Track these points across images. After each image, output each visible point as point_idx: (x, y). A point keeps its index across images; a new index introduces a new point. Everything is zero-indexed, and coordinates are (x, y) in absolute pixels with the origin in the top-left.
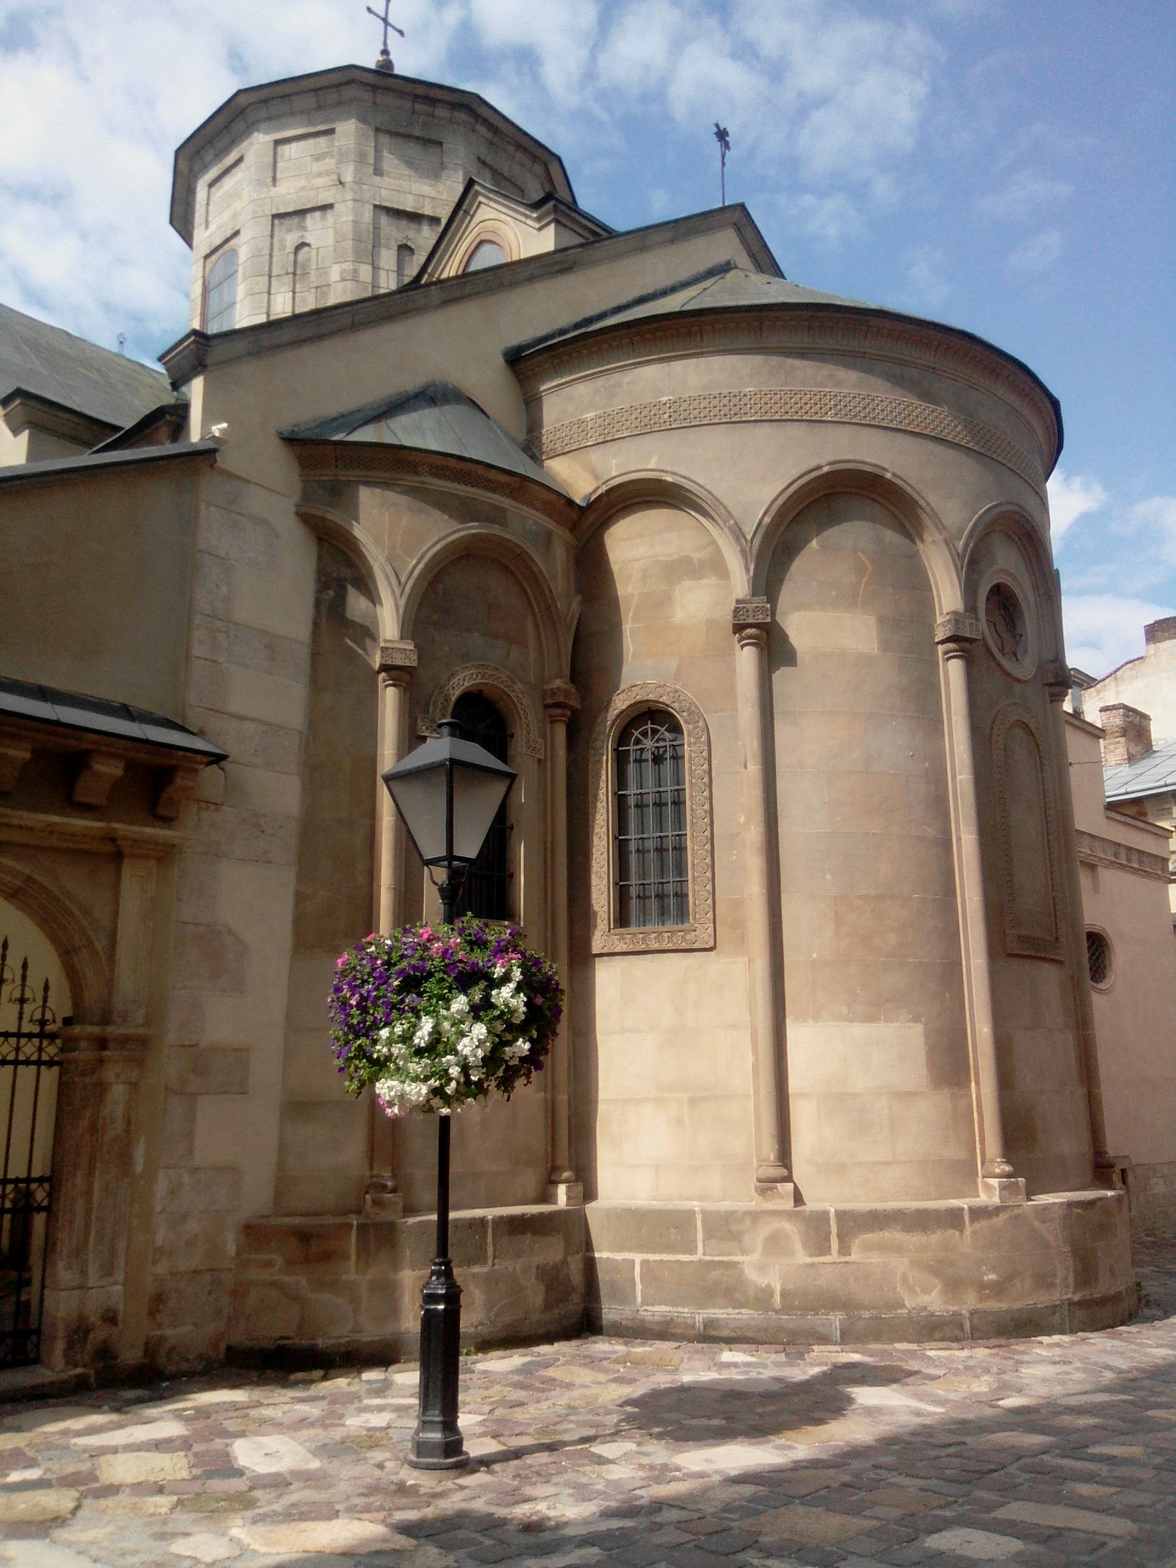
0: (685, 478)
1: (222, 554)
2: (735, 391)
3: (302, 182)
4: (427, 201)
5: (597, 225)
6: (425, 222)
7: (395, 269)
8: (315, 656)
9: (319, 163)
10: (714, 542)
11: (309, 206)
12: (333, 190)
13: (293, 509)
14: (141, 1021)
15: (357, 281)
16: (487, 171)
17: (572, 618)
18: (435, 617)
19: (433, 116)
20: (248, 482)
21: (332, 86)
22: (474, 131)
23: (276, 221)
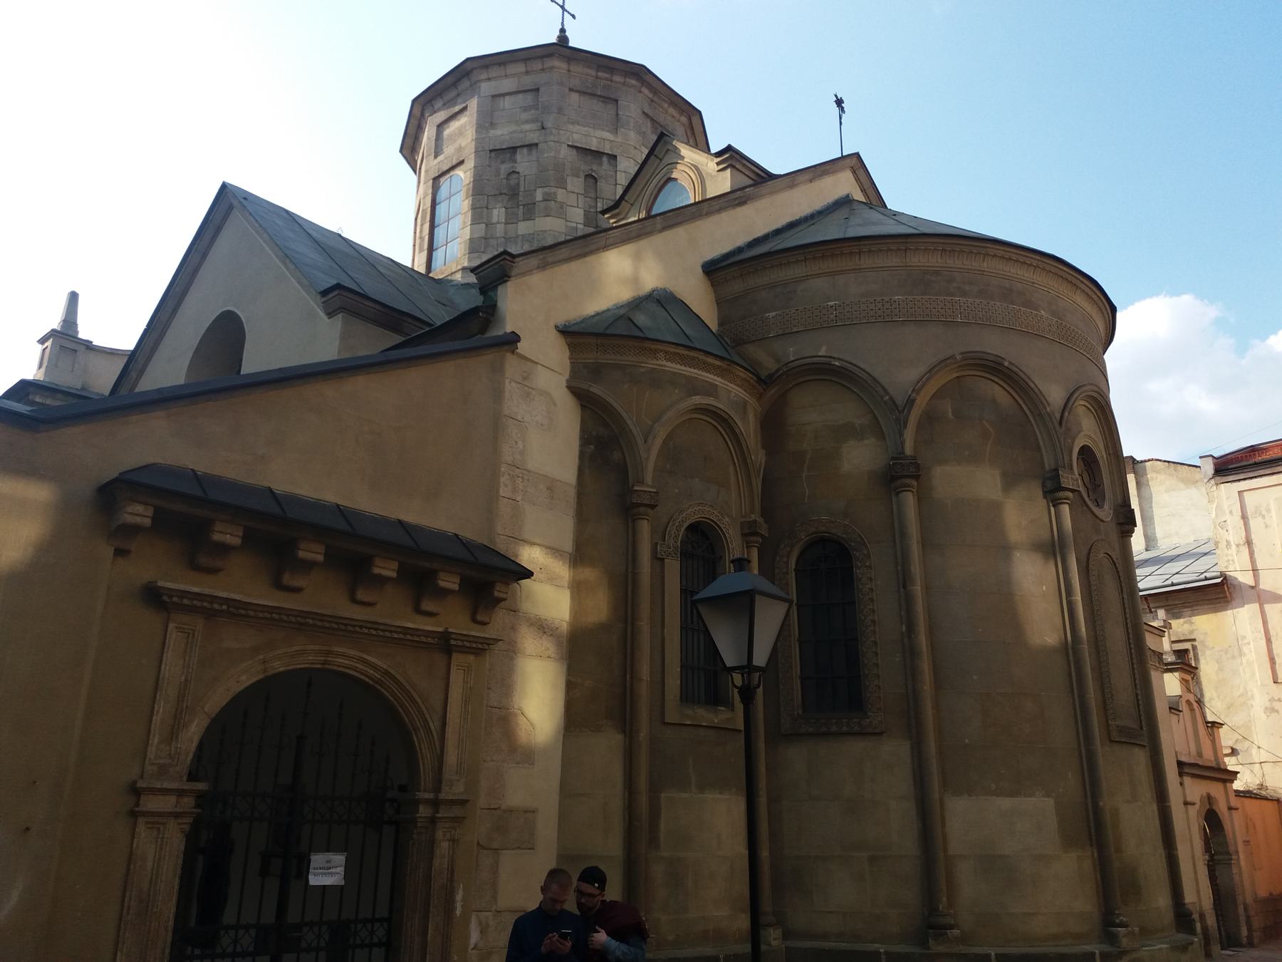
0: (850, 363)
1: (519, 418)
2: (887, 299)
3: (513, 128)
4: (607, 142)
5: (762, 171)
6: (605, 159)
7: (583, 192)
8: (581, 495)
10: (872, 412)
11: (519, 145)
12: (537, 134)
13: (564, 384)
14: (462, 789)
15: (556, 201)
16: (649, 120)
17: (760, 466)
18: (668, 466)
19: (611, 81)
20: (536, 363)
22: (640, 92)
23: (493, 154)
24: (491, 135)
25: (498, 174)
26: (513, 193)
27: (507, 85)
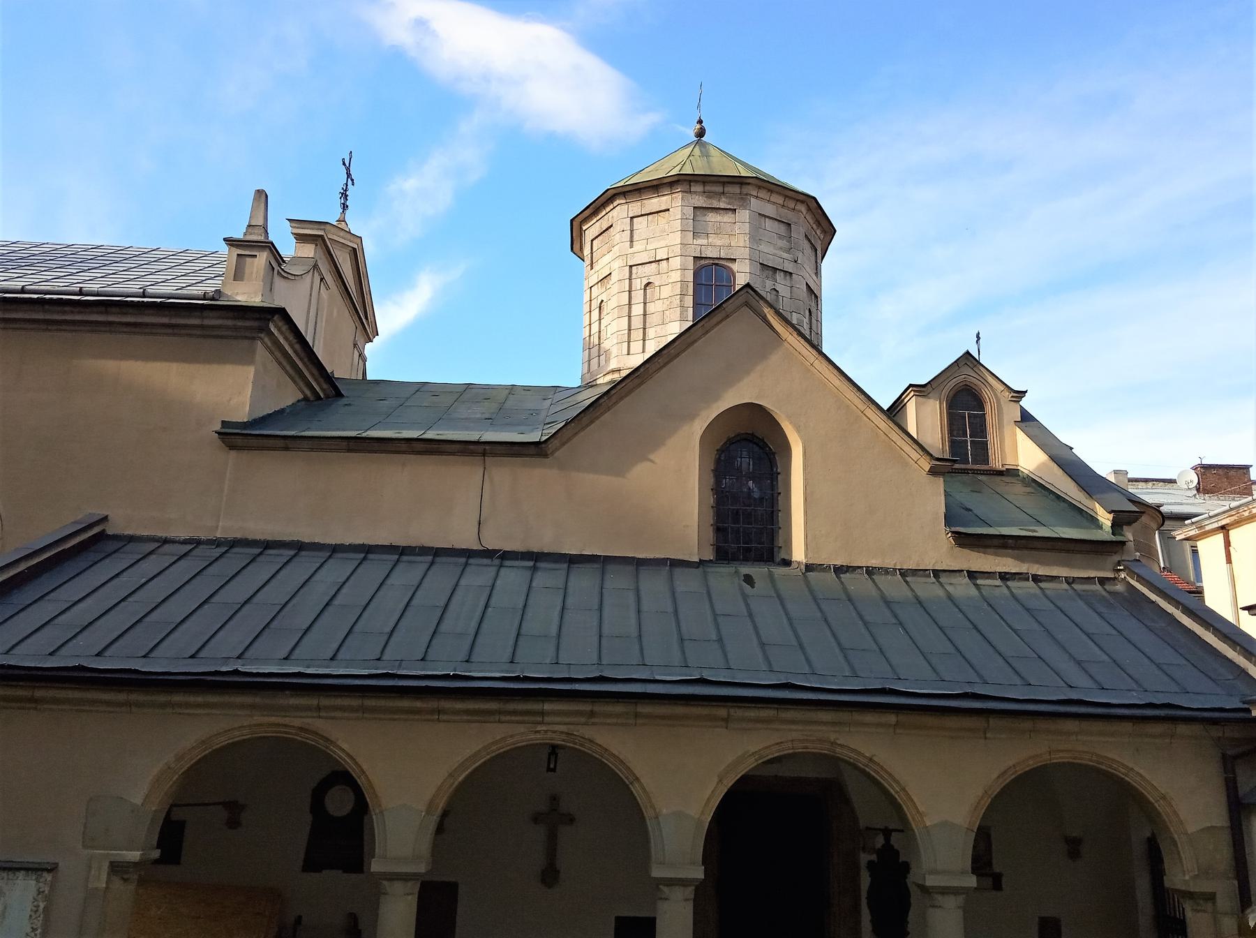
9: (781, 241)
21: (794, 199)
27: (770, 210)
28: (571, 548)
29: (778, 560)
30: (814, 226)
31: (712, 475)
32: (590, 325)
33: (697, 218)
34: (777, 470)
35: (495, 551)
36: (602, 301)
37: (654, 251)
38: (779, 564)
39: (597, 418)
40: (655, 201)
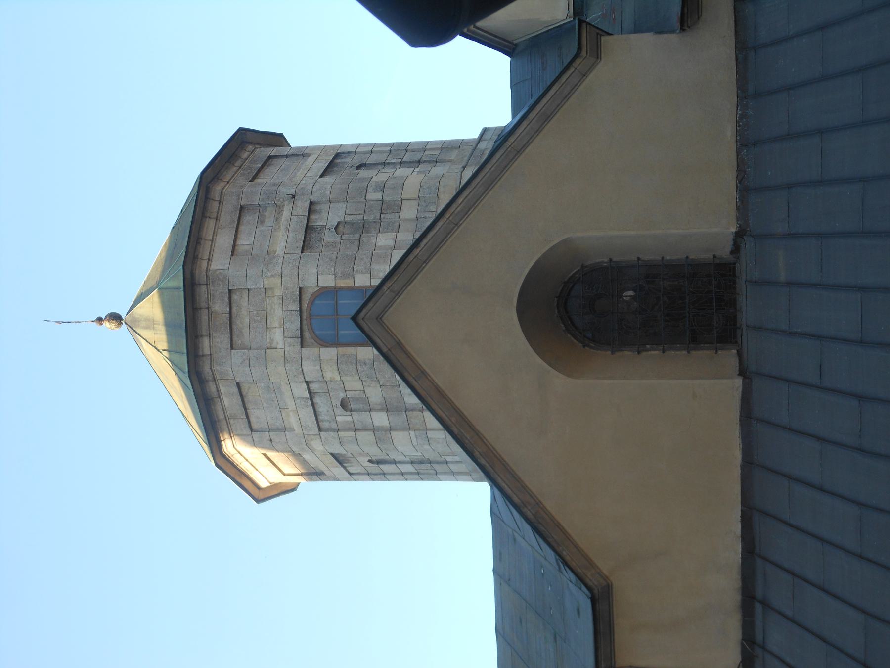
6: (338, 161)
9: (266, 220)
11: (305, 222)
12: (299, 203)
19: (246, 159)
24: (282, 254)
25: (334, 245)
26: (363, 227)
27: (224, 240)
28: (733, 553)
29: (731, 259)
30: (238, 164)
31: (618, 354)
32: (402, 474)
33: (247, 343)
34: (605, 262)
35: (744, 652)
36: (370, 461)
37: (298, 401)
38: (738, 258)
39: (553, 519)
40: (226, 401)
